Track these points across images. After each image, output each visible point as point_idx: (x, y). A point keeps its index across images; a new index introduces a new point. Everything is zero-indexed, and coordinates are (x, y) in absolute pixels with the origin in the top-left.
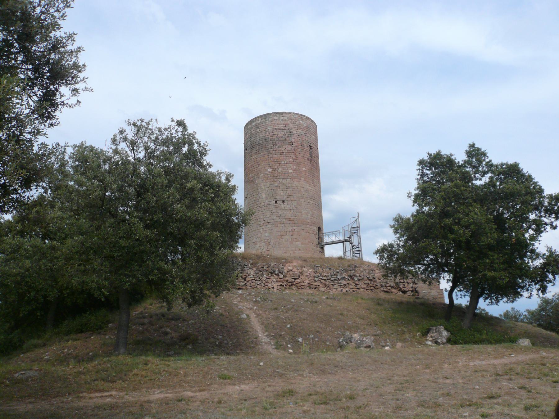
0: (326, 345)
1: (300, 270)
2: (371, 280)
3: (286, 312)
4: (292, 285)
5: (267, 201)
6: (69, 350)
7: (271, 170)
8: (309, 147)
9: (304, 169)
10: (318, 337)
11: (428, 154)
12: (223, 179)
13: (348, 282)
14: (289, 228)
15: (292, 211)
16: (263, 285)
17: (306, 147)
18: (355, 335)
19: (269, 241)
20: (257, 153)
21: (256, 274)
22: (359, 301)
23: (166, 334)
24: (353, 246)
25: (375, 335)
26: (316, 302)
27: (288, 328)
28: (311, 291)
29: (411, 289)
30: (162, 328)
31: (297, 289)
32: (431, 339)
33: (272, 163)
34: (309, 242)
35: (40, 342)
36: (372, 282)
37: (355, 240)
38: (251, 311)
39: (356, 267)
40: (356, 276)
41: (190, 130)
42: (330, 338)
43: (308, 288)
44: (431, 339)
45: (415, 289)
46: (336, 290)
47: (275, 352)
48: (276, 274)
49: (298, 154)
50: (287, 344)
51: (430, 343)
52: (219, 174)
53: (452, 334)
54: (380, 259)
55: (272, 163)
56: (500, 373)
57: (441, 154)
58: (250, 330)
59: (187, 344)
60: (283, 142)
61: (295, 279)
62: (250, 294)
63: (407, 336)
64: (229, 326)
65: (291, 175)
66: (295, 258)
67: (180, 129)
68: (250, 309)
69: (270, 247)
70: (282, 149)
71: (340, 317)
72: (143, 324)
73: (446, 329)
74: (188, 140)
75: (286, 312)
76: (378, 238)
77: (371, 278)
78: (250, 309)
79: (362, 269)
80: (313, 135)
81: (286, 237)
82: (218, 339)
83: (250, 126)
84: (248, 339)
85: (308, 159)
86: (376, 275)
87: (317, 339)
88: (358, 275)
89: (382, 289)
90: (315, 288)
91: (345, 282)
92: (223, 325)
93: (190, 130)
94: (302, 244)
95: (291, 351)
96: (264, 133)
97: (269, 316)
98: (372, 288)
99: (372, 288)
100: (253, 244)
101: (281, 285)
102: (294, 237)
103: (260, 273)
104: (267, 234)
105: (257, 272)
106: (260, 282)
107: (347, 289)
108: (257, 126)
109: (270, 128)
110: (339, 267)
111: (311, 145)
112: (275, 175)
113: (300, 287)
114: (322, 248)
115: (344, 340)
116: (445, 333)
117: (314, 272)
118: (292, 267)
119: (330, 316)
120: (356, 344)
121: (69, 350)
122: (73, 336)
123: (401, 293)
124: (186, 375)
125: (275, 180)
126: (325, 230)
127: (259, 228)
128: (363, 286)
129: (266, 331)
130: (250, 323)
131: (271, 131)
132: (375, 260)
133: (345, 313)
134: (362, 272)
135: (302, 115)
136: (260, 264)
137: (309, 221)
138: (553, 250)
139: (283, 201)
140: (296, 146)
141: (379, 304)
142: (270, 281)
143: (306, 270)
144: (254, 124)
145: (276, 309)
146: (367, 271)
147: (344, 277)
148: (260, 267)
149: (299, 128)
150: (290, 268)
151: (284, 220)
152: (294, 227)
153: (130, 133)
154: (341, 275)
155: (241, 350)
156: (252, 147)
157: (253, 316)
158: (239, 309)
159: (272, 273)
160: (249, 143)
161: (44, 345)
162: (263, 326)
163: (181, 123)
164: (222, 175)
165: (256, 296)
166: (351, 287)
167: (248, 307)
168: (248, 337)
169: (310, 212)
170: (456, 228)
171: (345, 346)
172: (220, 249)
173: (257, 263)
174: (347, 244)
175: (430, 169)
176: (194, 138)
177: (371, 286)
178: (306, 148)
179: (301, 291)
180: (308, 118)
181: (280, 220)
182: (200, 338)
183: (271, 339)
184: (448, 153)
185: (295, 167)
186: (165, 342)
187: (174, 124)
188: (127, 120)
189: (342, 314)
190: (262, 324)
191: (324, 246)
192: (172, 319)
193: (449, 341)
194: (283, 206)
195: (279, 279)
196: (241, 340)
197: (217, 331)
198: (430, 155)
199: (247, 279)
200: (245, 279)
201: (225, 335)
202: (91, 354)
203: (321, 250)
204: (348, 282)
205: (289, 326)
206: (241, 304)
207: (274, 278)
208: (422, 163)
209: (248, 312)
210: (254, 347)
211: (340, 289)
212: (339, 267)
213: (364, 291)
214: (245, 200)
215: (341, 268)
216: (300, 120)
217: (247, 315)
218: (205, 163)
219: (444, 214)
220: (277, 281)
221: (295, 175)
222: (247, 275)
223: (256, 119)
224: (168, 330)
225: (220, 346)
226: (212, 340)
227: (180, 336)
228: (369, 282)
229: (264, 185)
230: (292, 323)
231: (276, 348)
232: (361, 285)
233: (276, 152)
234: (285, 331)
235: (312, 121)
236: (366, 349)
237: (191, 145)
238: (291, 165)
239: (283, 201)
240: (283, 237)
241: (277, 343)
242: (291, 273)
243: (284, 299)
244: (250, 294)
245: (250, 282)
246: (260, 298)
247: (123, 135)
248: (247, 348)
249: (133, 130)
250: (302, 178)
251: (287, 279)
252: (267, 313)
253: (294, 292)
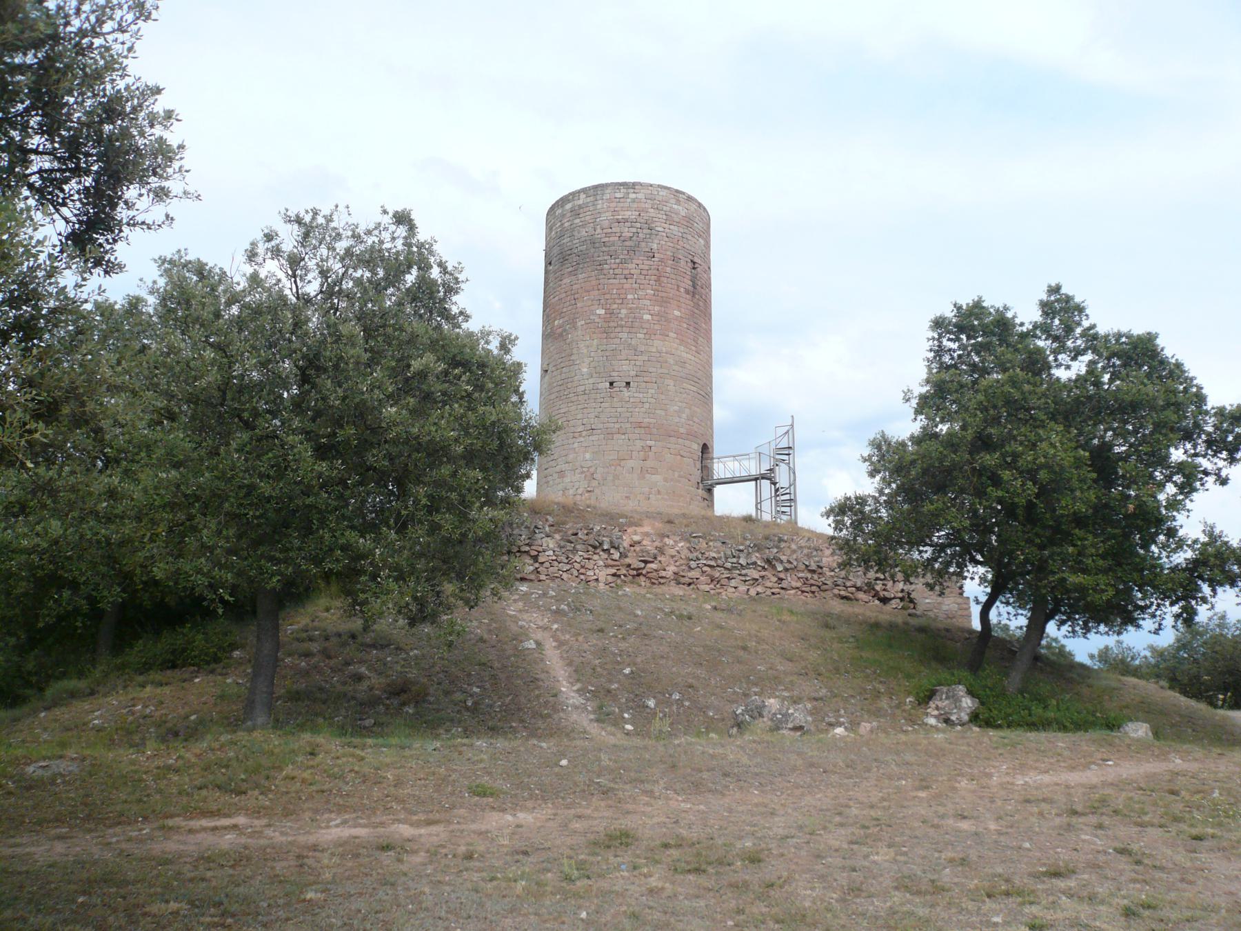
0: (708, 717)
1: (657, 544)
2: (813, 572)
3: (624, 638)
4: (638, 575)
5: (591, 381)
6: (145, 706)
7: (603, 312)
8: (690, 265)
9: (677, 313)
10: (689, 699)
11: (955, 305)
12: (494, 346)
13: (763, 573)
14: (639, 444)
15: (647, 406)
16: (576, 573)
17: (683, 263)
18: (772, 700)
19: (592, 470)
20: (573, 273)
21: (561, 548)
22: (784, 618)
23: (359, 678)
24: (777, 490)
25: (815, 699)
26: (690, 618)
27: (625, 675)
28: (679, 591)
29: (900, 595)
30: (349, 664)
31: (648, 584)
32: (936, 713)
33: (608, 296)
35: (82, 684)
36: (816, 577)
37: (782, 478)
38: (547, 634)
39: (781, 540)
40: (781, 562)
41: (422, 235)
42: (716, 703)
43: (673, 583)
44: (936, 713)
45: (909, 594)
46: (735, 591)
47: (594, 729)
48: (604, 550)
49: (665, 280)
50: (622, 712)
51: (932, 721)
52: (486, 334)
53: (982, 703)
54: (835, 529)
55: (608, 296)
56: (1079, 808)
57: (984, 304)
58: (542, 676)
59: (404, 704)
60: (632, 251)
61: (646, 562)
62: (545, 594)
63: (884, 703)
64: (496, 665)
65: (647, 326)
66: (649, 516)
67: (402, 231)
68: (545, 628)
69: (595, 483)
70: (630, 266)
71: (741, 653)
72: (307, 655)
73: (971, 693)
74: (418, 256)
75: (624, 638)
76: (834, 477)
77: (813, 567)
78: (545, 628)
79: (794, 547)
80: (700, 236)
81: (631, 463)
82: (471, 696)
83: (559, 211)
84: (538, 697)
85: (687, 292)
86: (824, 560)
87: (687, 704)
88: (784, 558)
89: (836, 591)
90: (689, 584)
91: (755, 574)
92: (484, 664)
93: (422, 235)
94: (666, 480)
95: (629, 727)
96: (590, 228)
97: (586, 646)
98: (814, 588)
99: (814, 588)
100: (556, 476)
101: (614, 575)
102: (649, 463)
103: (570, 546)
104: (588, 456)
105: (562, 543)
106: (568, 567)
107: (760, 589)
108: (575, 213)
109: (605, 218)
110: (745, 539)
111: (696, 260)
112: (612, 324)
113: (657, 580)
114: (710, 491)
115: (746, 711)
116: (968, 702)
117: (689, 549)
118: (642, 535)
119: (719, 651)
120: (772, 720)
121: (145, 706)
122: (156, 676)
123: (877, 602)
124: (398, 783)
125: (612, 335)
126: (718, 449)
127: (571, 441)
128: (794, 584)
129: (578, 680)
130: (542, 660)
131: (606, 224)
132: (825, 527)
133: (752, 644)
134: (794, 551)
135: (677, 191)
136: (570, 527)
137: (682, 430)
138: (1217, 531)
139: (628, 384)
140: (661, 260)
141: (826, 626)
142: (590, 564)
143: (672, 542)
144: (568, 206)
145: (601, 630)
146: (806, 551)
147: (755, 563)
148: (570, 532)
149: (669, 219)
150: (636, 538)
151: (628, 425)
152: (649, 443)
153: (289, 238)
154: (747, 558)
155: (522, 721)
156: (563, 259)
157: (550, 644)
158: (521, 627)
159: (595, 547)
160: (556, 251)
161: (92, 693)
162: (570, 669)
163: (402, 218)
164: (491, 338)
165: (559, 600)
166: (769, 585)
167: (541, 624)
168: (537, 692)
169: (687, 411)
170: (1006, 475)
171: (749, 723)
172: (481, 508)
173: (564, 523)
174: (765, 484)
175: (958, 339)
176: (431, 252)
177: (812, 585)
178: (685, 266)
179: (657, 589)
180: (690, 199)
181: (617, 426)
182: (431, 691)
183: (587, 700)
184: (999, 305)
185: (657, 308)
186: (354, 698)
187: (387, 220)
188: (283, 211)
189: (744, 648)
190: (570, 664)
191: (712, 486)
192: (374, 646)
193: (975, 718)
194: (626, 393)
195: (610, 562)
196: (523, 700)
197: (469, 675)
198: (959, 308)
199: (541, 559)
200: (535, 558)
201: (487, 686)
202: (193, 718)
203: (705, 495)
204: (763, 573)
205: (627, 671)
206: (525, 616)
207: (600, 559)
208: (938, 324)
209: (539, 635)
210: (549, 716)
211: (743, 588)
212: (745, 539)
213: (795, 595)
214: (542, 377)
215: (748, 543)
216: (673, 201)
217: (538, 643)
218: (455, 310)
219: (983, 443)
220: (607, 566)
221: (656, 327)
222: (540, 549)
223: (574, 195)
224: (363, 670)
225: (474, 710)
226: (458, 696)
227: (389, 685)
228: (809, 576)
229: (586, 347)
230: (635, 664)
231: (597, 720)
232: (791, 580)
233: (617, 271)
234: (619, 682)
235: (700, 205)
236: (792, 733)
237: (425, 267)
238: (648, 303)
239: (628, 384)
240: (622, 463)
241: (601, 707)
242: (637, 548)
243: (620, 609)
244: (545, 594)
245: (547, 564)
246: (568, 605)
247: (273, 243)
248: (533, 717)
249: (295, 233)
250: (671, 334)
251: (628, 561)
252: (581, 638)
253: (643, 591)
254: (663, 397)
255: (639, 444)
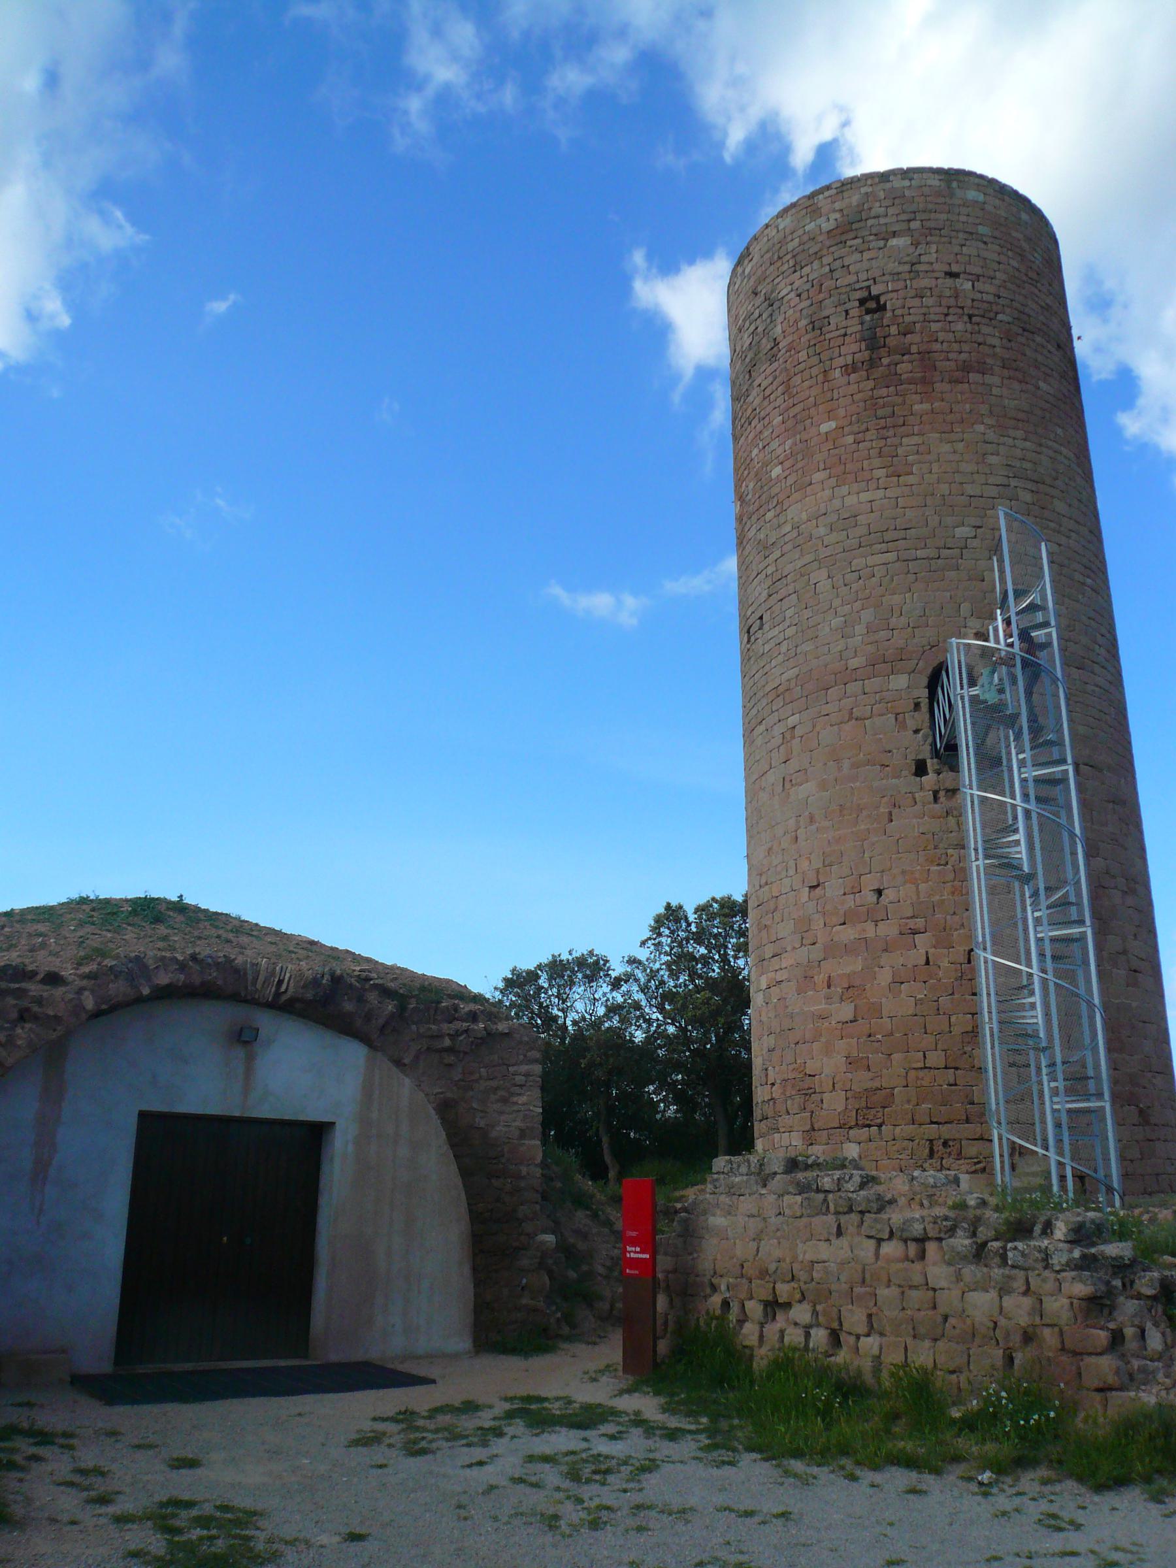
15: (784, 648)
34: (856, 766)
81: (771, 777)
102: (793, 765)
111: (875, 291)
137: (854, 663)
152: (792, 721)
239: (761, 618)
254: (807, 613)
255: (778, 730)
